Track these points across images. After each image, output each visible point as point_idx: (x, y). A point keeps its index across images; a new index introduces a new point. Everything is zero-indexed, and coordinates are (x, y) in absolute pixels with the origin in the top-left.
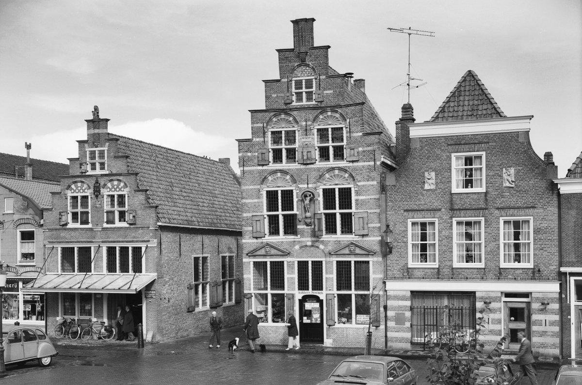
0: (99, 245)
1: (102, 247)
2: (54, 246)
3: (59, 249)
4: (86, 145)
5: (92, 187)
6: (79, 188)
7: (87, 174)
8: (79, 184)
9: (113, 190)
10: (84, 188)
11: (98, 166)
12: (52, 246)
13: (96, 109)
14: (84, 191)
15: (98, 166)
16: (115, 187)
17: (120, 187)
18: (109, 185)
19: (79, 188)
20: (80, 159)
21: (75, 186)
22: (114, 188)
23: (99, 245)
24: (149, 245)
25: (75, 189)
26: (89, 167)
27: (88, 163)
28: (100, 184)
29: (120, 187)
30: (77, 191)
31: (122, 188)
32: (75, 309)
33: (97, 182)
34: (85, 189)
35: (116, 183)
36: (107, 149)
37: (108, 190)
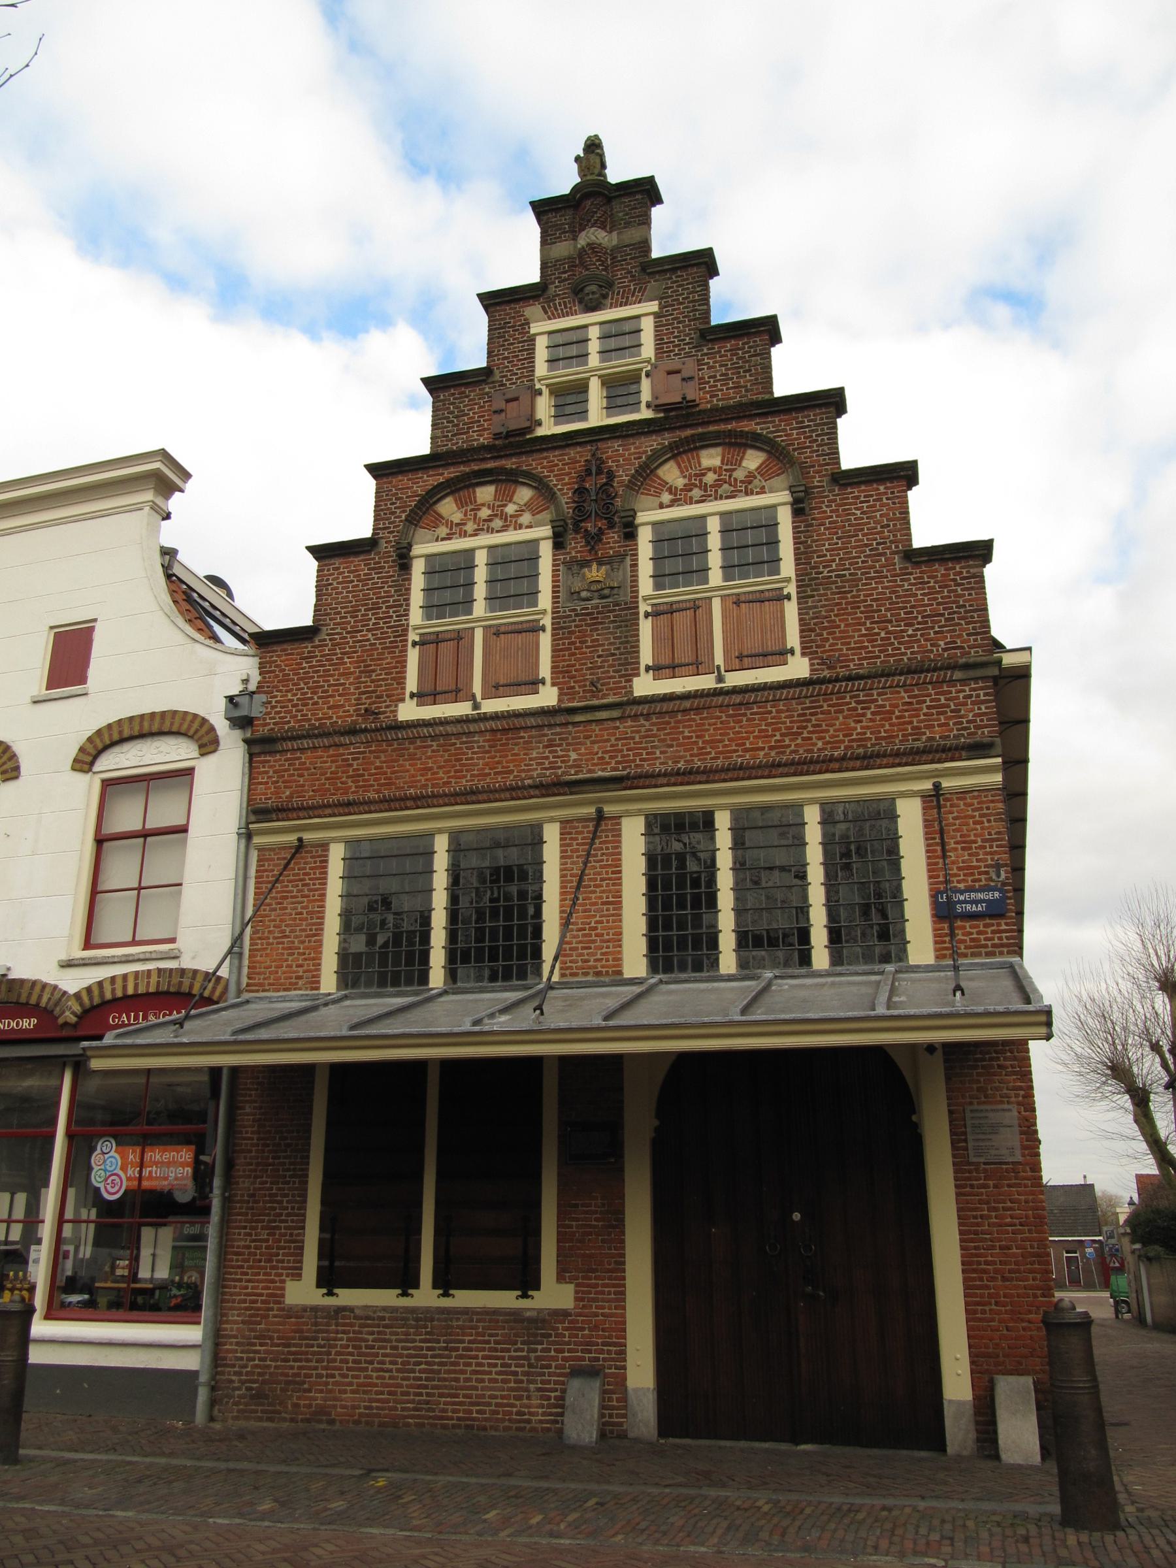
0: (600, 811)
1: (617, 819)
2: (307, 836)
3: (337, 855)
4: (533, 310)
5: (565, 499)
6: (485, 513)
7: (541, 432)
8: (485, 493)
9: (696, 493)
10: (510, 509)
11: (596, 395)
12: (292, 838)
13: (593, 147)
14: (511, 523)
15: (596, 395)
16: (710, 478)
17: (740, 474)
18: (671, 473)
19: (485, 513)
20: (497, 376)
21: (461, 504)
22: (704, 487)
23: (600, 811)
24: (946, 783)
25: (457, 517)
26: (544, 407)
27: (538, 386)
28: (611, 475)
29: (740, 474)
30: (470, 527)
31: (751, 477)
32: (418, 1231)
33: (597, 467)
34: (520, 512)
35: (711, 458)
36: (653, 306)
37: (666, 497)
